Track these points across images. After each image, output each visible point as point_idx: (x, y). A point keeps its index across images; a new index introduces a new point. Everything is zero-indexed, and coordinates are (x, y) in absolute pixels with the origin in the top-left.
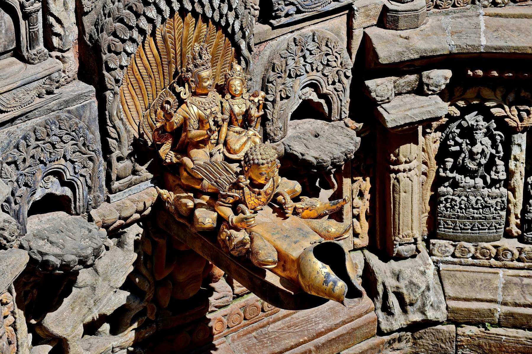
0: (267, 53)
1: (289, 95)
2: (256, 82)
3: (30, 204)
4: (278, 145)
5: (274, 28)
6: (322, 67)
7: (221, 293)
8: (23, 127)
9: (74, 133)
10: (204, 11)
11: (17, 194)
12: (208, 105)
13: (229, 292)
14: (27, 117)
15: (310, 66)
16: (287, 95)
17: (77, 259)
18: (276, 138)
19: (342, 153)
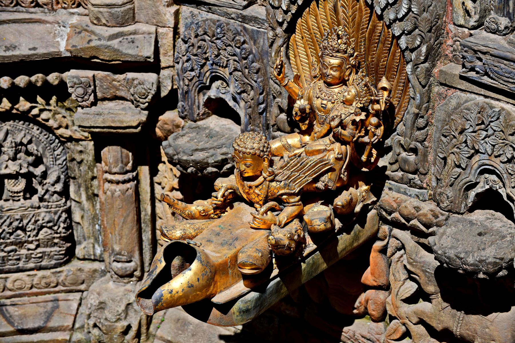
0: (454, 102)
1: (462, 165)
2: (437, 127)
3: (206, 97)
4: (442, 215)
5: (462, 78)
6: (506, 160)
7: (369, 335)
8: (204, 16)
9: (238, 50)
10: (372, 4)
11: (185, 75)
12: (323, 96)
13: (378, 340)
14: (210, 8)
15: (491, 147)
16: (460, 164)
17: (176, 157)
18: (441, 205)
19: (456, 256)
